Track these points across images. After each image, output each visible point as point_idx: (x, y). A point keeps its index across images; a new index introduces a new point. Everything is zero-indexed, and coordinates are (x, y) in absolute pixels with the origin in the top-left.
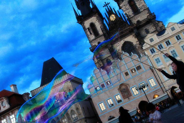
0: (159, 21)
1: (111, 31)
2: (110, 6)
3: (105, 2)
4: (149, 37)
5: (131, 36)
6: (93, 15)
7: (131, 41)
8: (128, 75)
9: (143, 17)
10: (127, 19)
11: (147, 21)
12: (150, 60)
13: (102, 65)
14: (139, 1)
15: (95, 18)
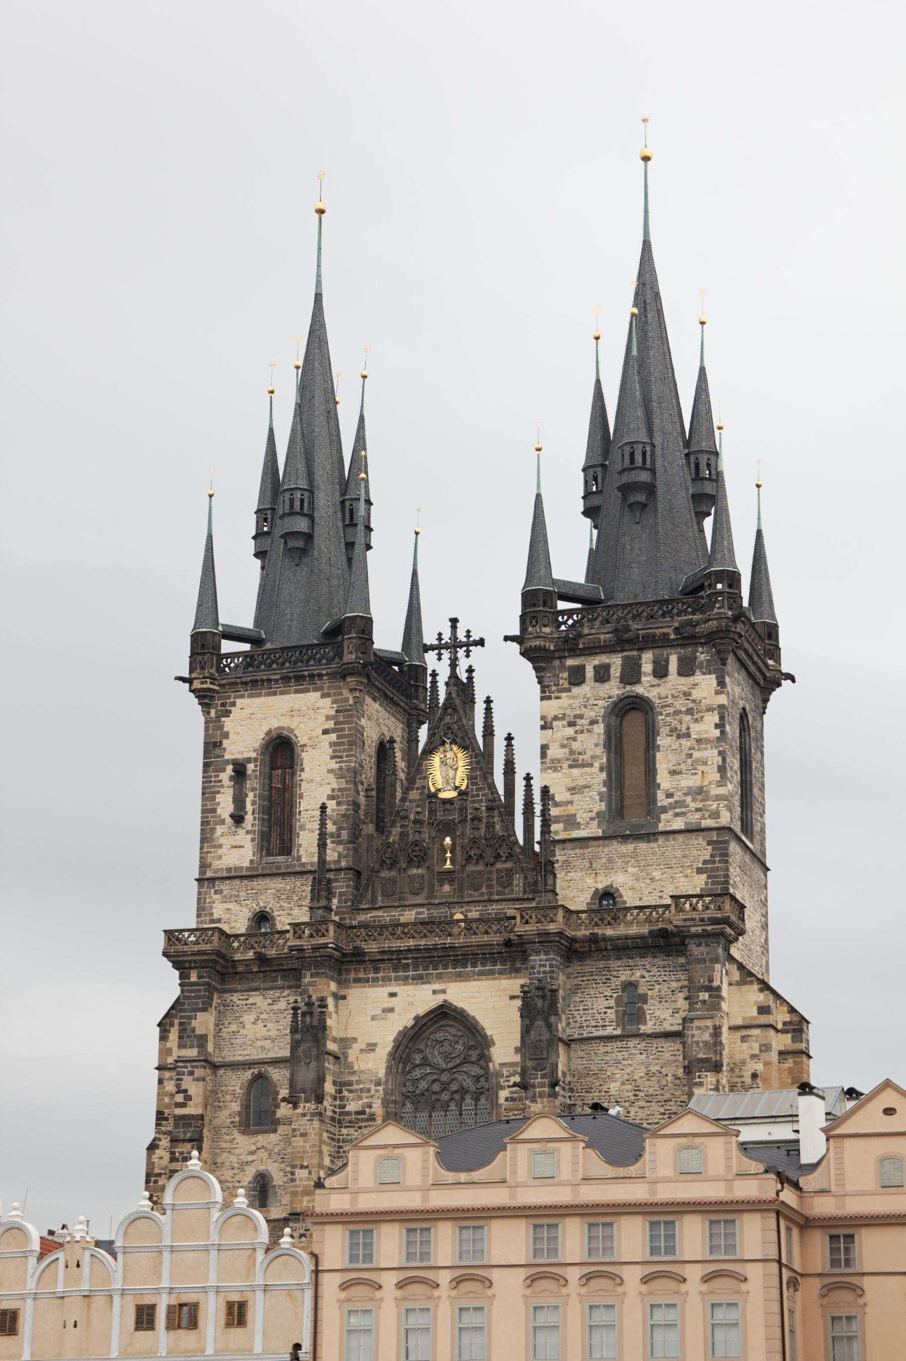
0: (751, 974)
2: (470, 670)
3: (454, 621)
4: (384, 1147)
5: (514, 984)
6: (320, 676)
7: (480, 1021)
8: (153, 1329)
9: (652, 880)
10: (537, 837)
11: (664, 934)
13: (192, 1110)
15: (327, 706)
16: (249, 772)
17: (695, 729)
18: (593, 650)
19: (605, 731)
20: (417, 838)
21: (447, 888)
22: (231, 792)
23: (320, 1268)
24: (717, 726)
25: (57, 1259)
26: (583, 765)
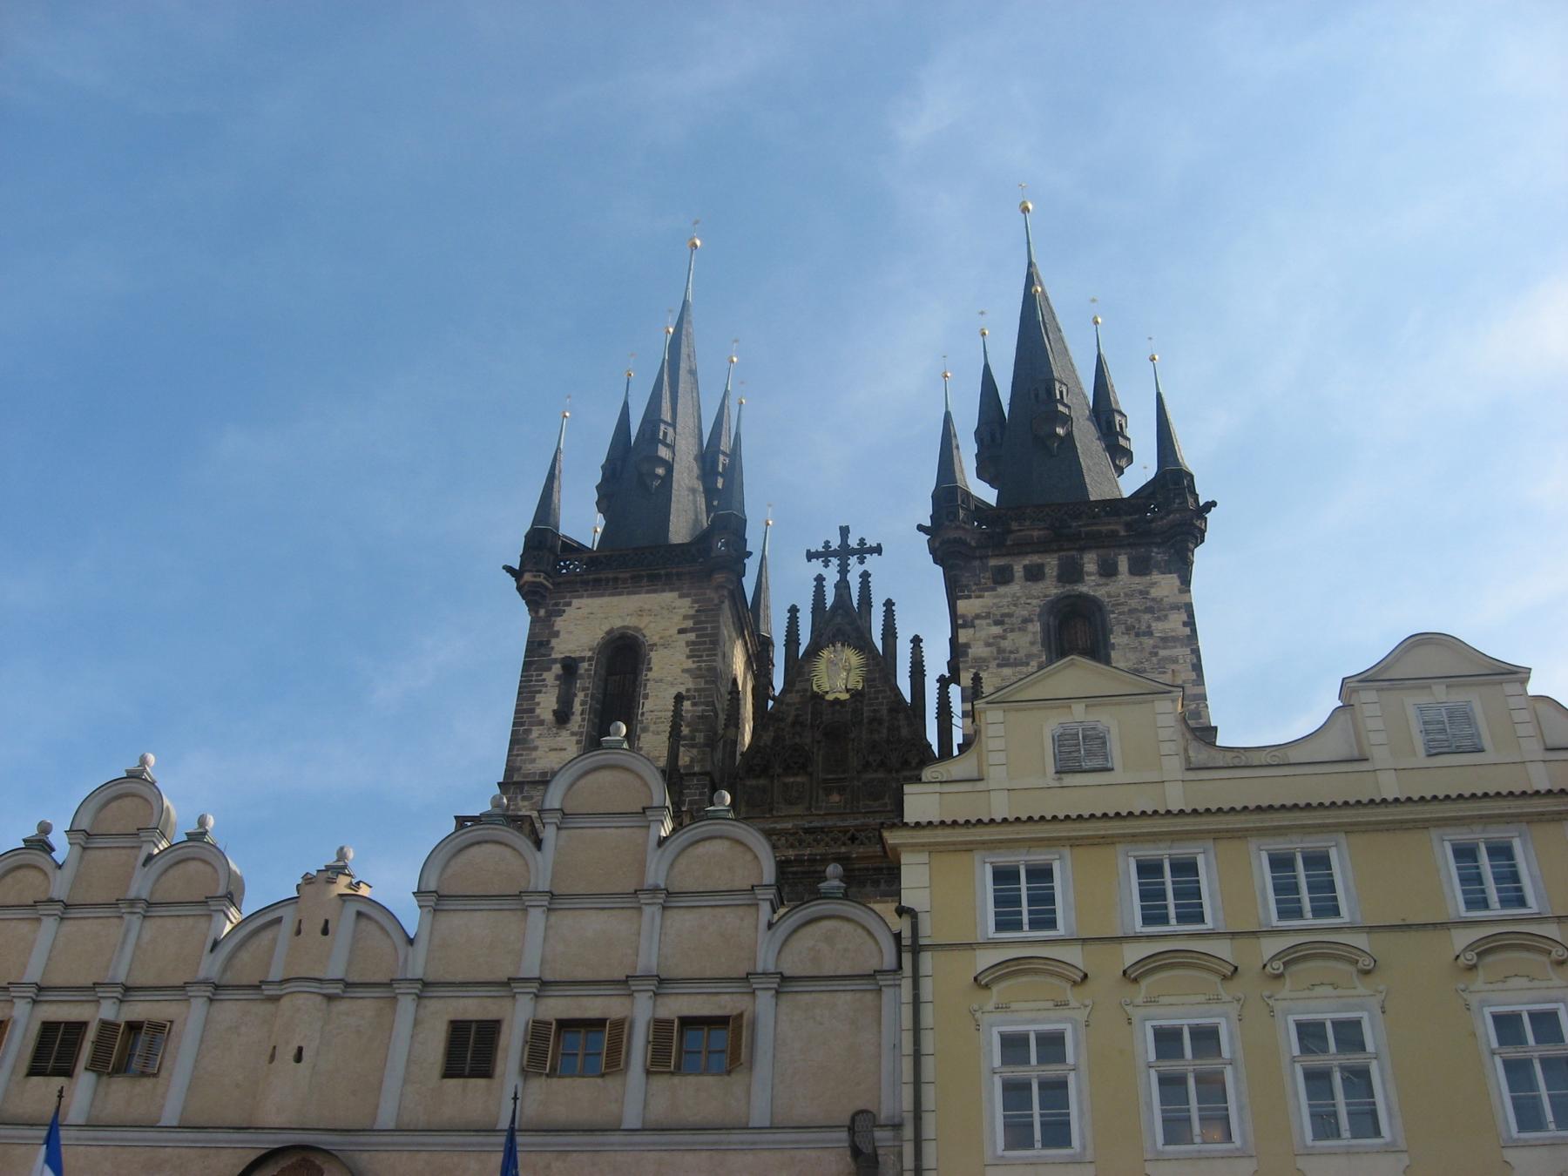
1: (759, 777)
2: (865, 576)
3: (845, 531)
6: (679, 576)
10: (957, 738)
12: (916, 1002)
14: (1148, 642)
16: (581, 671)
17: (1159, 628)
18: (1022, 548)
19: (1043, 630)
20: (797, 740)
21: (835, 798)
22: (557, 691)
23: (922, 941)
24: (1185, 624)
25: (279, 920)
26: (1016, 664)
